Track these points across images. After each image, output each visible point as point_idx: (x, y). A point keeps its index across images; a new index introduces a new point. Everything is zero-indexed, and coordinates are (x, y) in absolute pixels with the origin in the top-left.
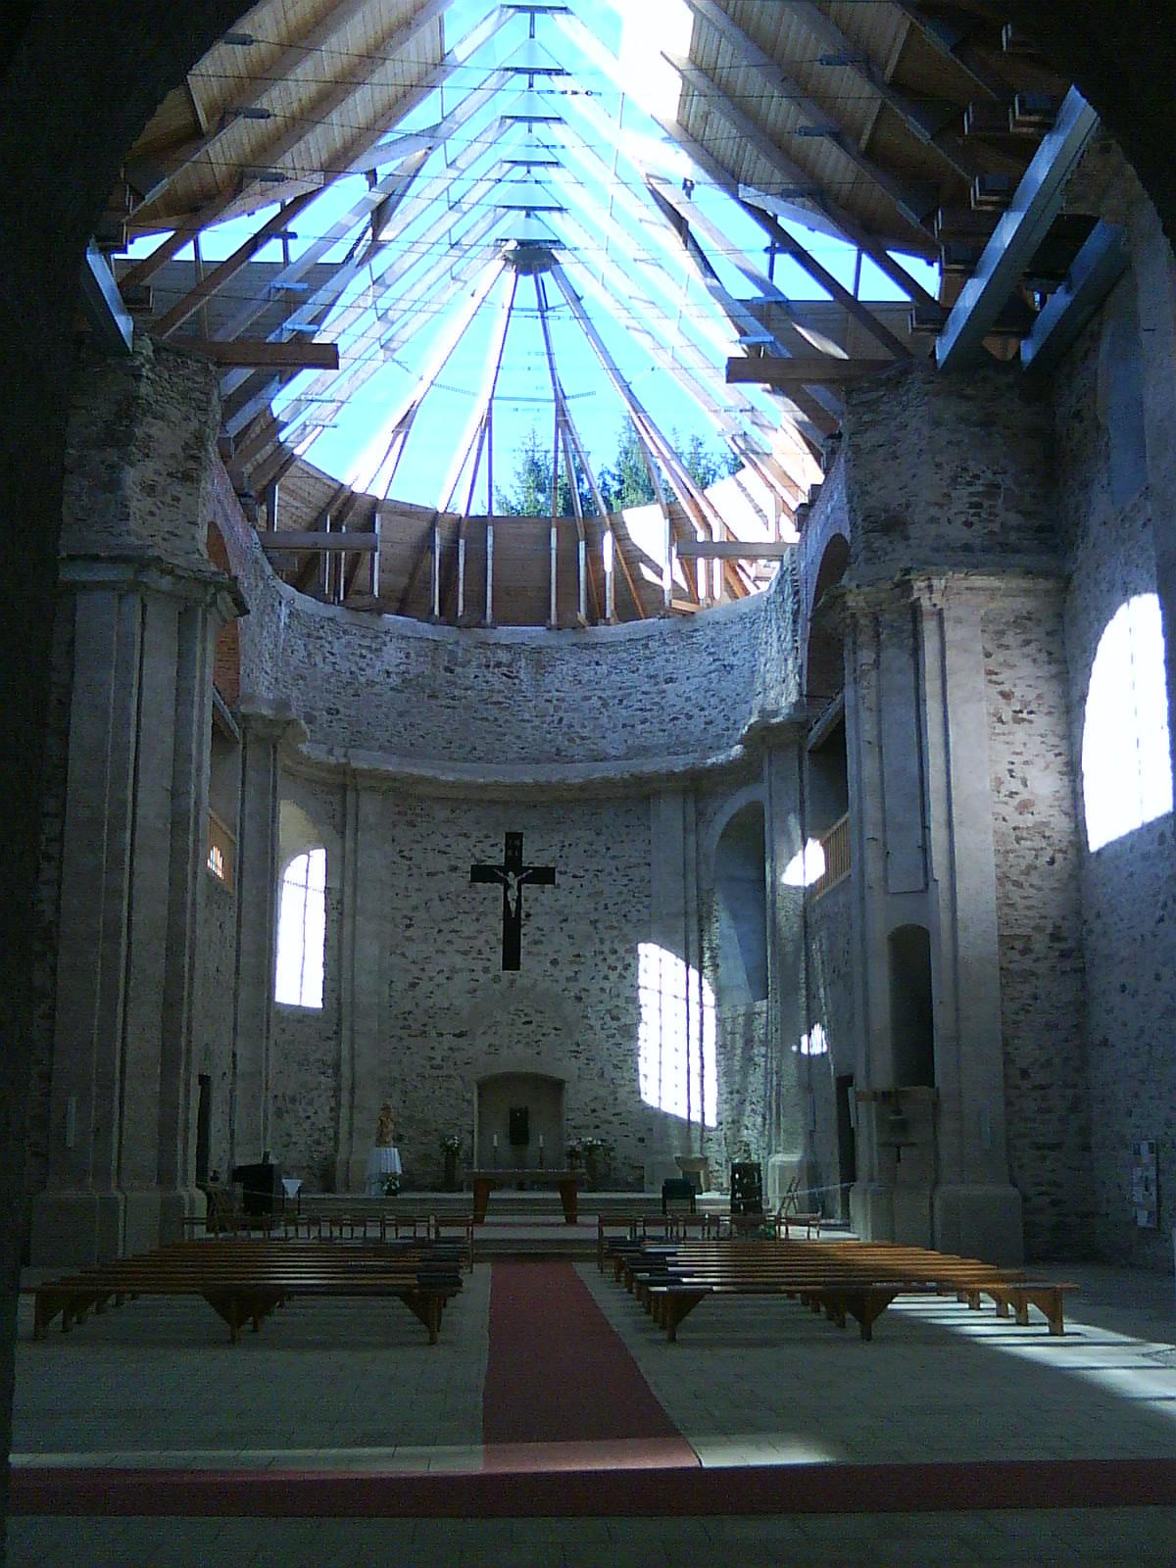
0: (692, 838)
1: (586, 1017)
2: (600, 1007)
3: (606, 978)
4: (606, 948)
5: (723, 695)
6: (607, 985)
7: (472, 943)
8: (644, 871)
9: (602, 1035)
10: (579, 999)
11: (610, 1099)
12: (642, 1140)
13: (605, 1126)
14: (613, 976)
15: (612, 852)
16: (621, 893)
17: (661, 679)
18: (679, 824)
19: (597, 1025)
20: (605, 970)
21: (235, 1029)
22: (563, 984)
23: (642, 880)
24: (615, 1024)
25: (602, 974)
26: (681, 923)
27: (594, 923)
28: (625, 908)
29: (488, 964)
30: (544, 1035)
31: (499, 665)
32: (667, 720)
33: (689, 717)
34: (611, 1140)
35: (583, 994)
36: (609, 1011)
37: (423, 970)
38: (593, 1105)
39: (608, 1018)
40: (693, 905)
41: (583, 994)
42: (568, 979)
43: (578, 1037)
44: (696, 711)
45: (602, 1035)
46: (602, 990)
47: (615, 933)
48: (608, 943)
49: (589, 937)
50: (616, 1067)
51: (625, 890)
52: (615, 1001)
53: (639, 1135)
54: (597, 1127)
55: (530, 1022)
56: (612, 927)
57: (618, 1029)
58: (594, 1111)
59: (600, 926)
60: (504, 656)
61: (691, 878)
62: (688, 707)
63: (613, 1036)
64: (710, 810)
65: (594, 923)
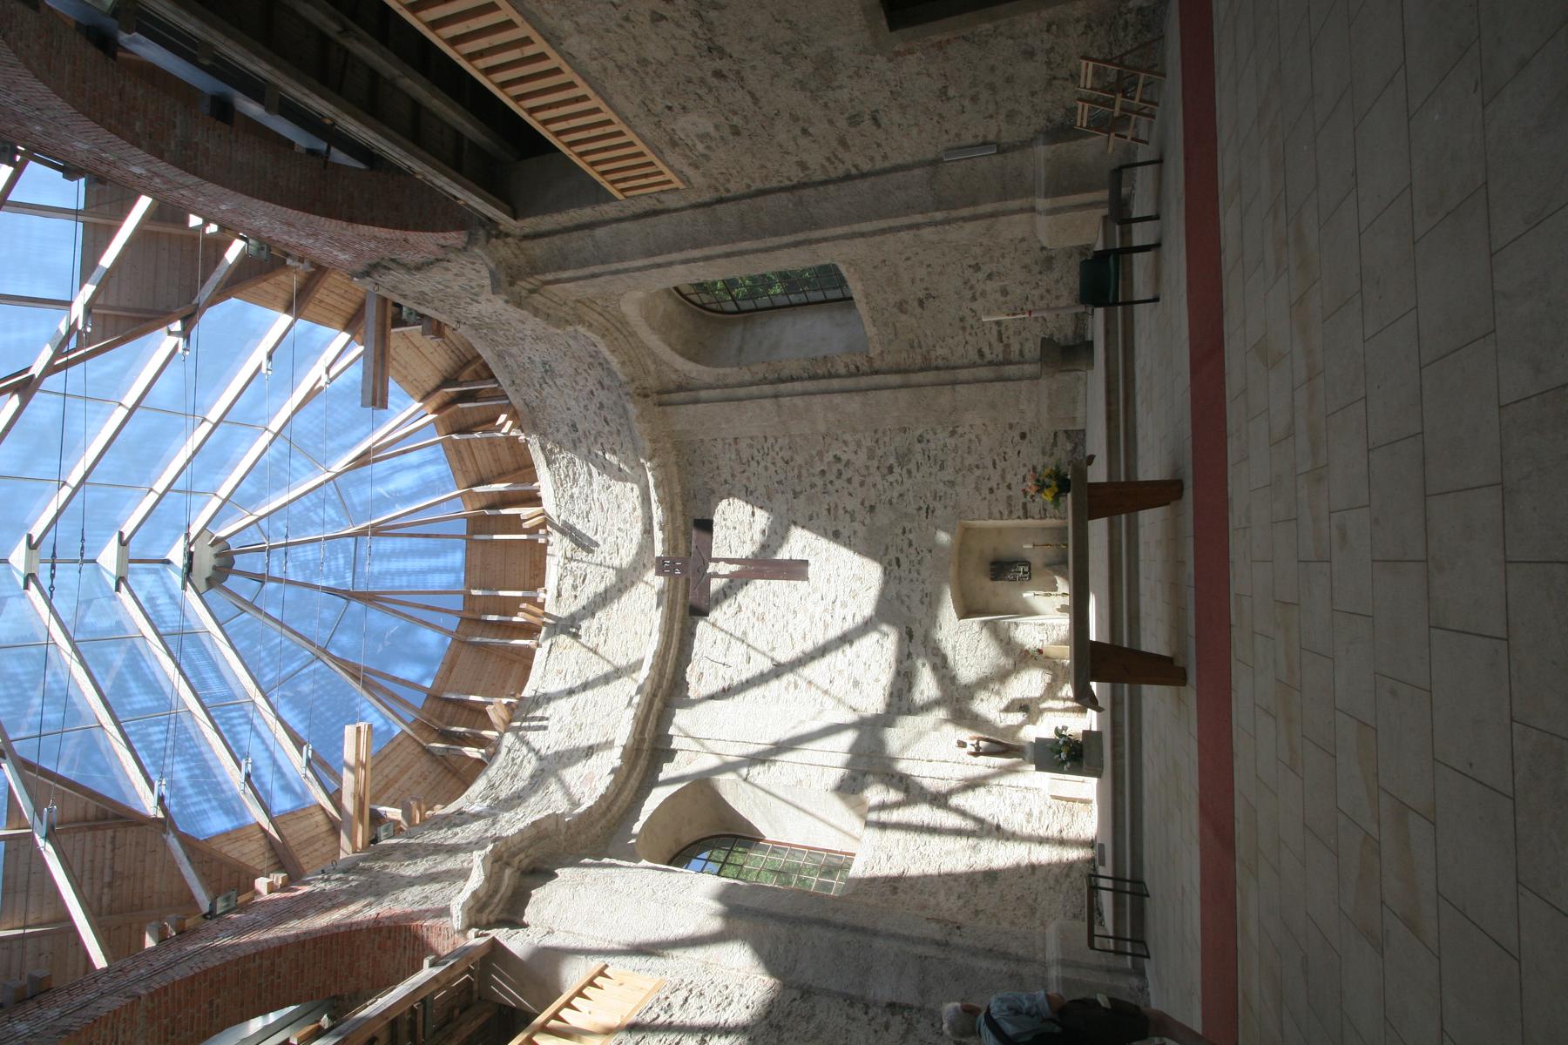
0: (703, 394)
1: (891, 503)
2: (880, 487)
3: (849, 481)
4: (819, 482)
5: (571, 371)
6: (856, 480)
7: (817, 618)
8: (743, 444)
9: (908, 483)
10: (872, 508)
11: (978, 472)
12: (1023, 436)
13: (1009, 478)
14: (847, 474)
15: (729, 479)
16: (766, 468)
17: (575, 436)
18: (691, 407)
19: (898, 489)
20: (839, 484)
21: (851, 1001)
22: (856, 525)
23: (751, 446)
24: (897, 470)
25: (846, 485)
26: (785, 401)
27: (796, 495)
28: (780, 463)
29: (838, 603)
30: (910, 545)
31: (575, 587)
32: (607, 429)
33: (601, 406)
34: (1023, 471)
35: (867, 504)
36: (883, 477)
37: (840, 672)
38: (985, 492)
39: (891, 478)
40: (767, 389)
41: (867, 504)
42: (853, 520)
43: (911, 510)
44: (596, 401)
45: (908, 483)
46: (862, 484)
47: (804, 472)
48: (815, 480)
49: (810, 500)
50: (942, 467)
51: (763, 464)
52: (873, 470)
53: (1017, 438)
54: (1009, 487)
55: (898, 560)
56: (799, 476)
57: (901, 465)
58: (991, 491)
59: (798, 489)
60: (569, 581)
61: (742, 392)
62: (593, 407)
63: (909, 472)
64: (674, 377)
65: (796, 495)
